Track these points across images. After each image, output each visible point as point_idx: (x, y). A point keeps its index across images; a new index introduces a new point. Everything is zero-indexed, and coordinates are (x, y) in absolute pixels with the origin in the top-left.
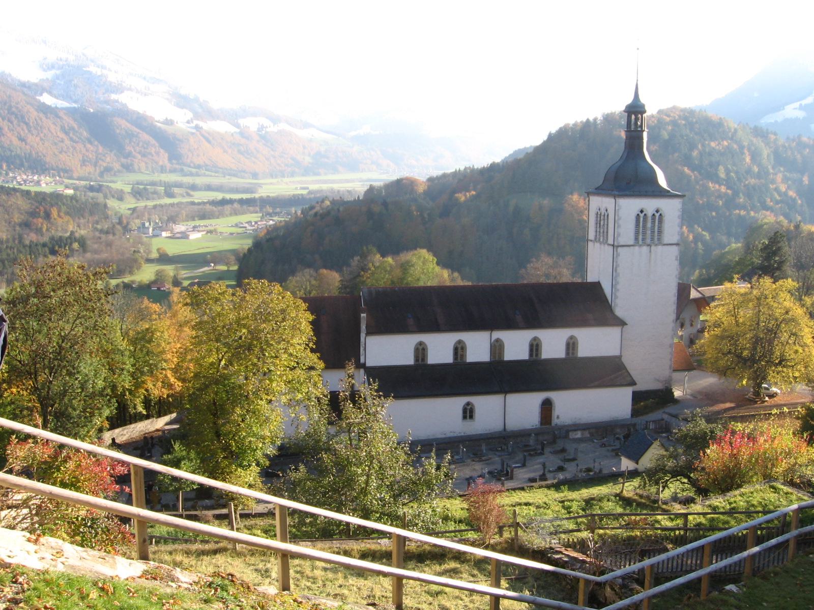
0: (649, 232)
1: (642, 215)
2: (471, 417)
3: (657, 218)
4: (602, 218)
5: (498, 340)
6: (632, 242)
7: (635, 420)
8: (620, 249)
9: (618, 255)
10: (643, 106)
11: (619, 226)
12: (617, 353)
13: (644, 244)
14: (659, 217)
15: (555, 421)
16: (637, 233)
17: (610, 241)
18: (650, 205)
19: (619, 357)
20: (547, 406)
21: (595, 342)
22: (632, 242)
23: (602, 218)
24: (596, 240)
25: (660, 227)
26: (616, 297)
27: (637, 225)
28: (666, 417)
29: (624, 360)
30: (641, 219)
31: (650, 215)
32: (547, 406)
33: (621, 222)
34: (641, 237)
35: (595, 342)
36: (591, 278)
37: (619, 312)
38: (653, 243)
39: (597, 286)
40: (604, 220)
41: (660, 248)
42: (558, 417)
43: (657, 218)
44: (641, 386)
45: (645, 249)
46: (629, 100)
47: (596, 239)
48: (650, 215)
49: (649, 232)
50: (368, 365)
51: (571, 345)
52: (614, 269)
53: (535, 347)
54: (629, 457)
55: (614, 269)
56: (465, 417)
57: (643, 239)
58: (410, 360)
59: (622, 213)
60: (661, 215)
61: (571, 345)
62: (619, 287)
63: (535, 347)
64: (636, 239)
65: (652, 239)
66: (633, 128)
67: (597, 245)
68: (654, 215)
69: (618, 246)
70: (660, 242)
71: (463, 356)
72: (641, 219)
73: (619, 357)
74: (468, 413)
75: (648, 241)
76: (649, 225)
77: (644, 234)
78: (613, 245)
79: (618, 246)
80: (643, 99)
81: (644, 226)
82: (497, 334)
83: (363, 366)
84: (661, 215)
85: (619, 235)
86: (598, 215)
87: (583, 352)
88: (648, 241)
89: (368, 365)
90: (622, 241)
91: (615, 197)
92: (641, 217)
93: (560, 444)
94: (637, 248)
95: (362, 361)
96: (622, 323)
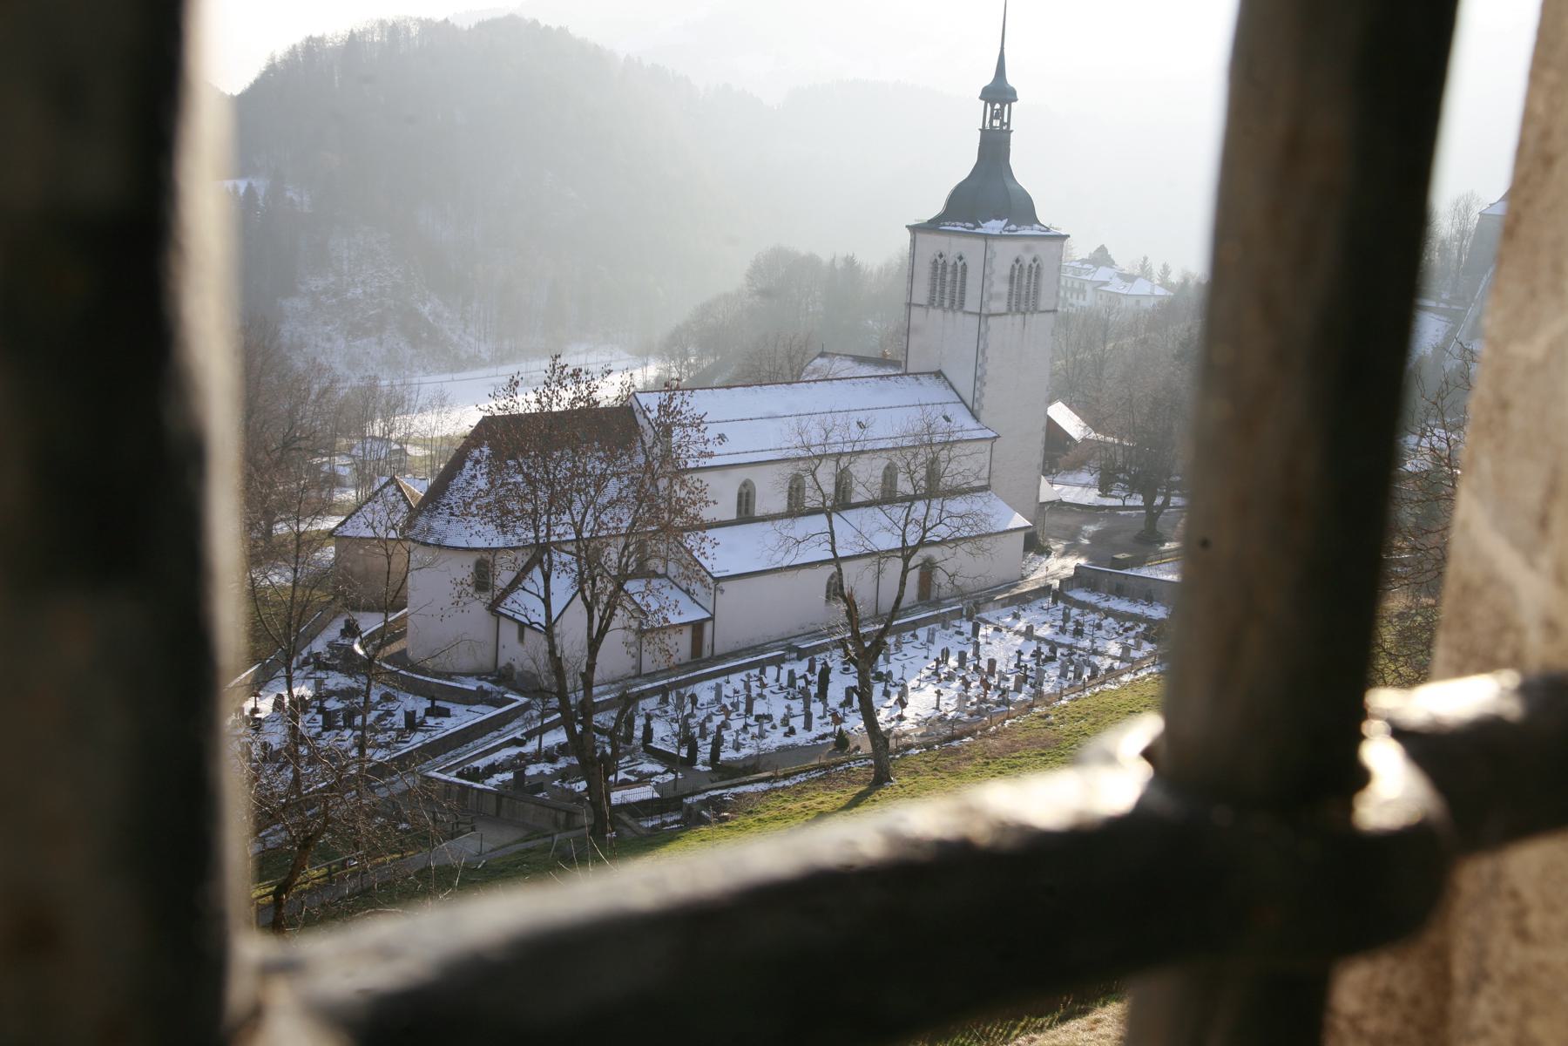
4: (949, 269)
8: (991, 320)
9: (988, 328)
10: (1013, 92)
13: (1018, 311)
17: (972, 304)
22: (1004, 309)
25: (1036, 284)
40: (955, 275)
45: (1019, 318)
46: (988, 78)
52: (980, 352)
55: (980, 352)
57: (1018, 303)
69: (988, 316)
70: (1036, 310)
76: (1025, 282)
78: (980, 314)
79: (988, 316)
80: (1011, 79)
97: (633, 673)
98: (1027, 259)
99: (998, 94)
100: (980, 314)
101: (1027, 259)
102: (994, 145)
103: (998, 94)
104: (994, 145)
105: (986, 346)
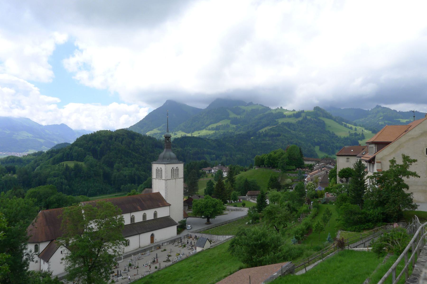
2: (128, 245)
5: (133, 216)
7: (179, 236)
14: (177, 169)
15: (155, 241)
16: (172, 175)
17: (164, 178)
18: (175, 166)
20: (152, 236)
21: (162, 212)
23: (159, 172)
24: (157, 178)
27: (172, 172)
28: (190, 233)
29: (171, 216)
32: (152, 236)
35: (162, 212)
36: (155, 190)
37: (168, 202)
39: (158, 194)
45: (174, 180)
47: (156, 177)
51: (155, 214)
53: (144, 216)
54: (200, 246)
55: (166, 187)
61: (155, 214)
63: (144, 216)
75: (175, 177)
76: (175, 172)
77: (174, 175)
82: (133, 214)
86: (157, 170)
87: (159, 216)
88: (175, 177)
91: (165, 164)
93: (163, 248)
96: (170, 205)
98: (175, 168)
101: (175, 168)
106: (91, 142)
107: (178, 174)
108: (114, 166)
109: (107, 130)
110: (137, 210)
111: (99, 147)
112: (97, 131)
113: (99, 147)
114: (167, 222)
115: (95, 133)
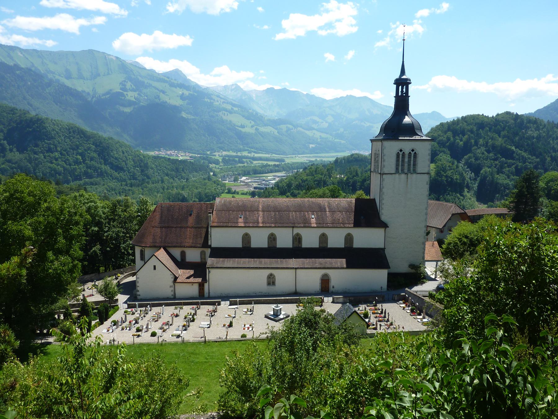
0: (406, 165)
1: (401, 153)
2: (274, 283)
3: (412, 155)
5: (298, 234)
6: (394, 172)
8: (384, 176)
9: (383, 180)
11: (384, 161)
12: (382, 246)
14: (413, 155)
16: (397, 165)
19: (383, 250)
22: (394, 172)
25: (415, 162)
26: (382, 209)
29: (386, 252)
30: (401, 156)
31: (407, 153)
33: (385, 158)
34: (400, 168)
35: (367, 238)
38: (410, 172)
41: (415, 175)
42: (333, 287)
43: (412, 155)
44: (394, 270)
45: (403, 176)
48: (407, 153)
49: (406, 165)
50: (212, 246)
56: (269, 284)
58: (239, 245)
59: (385, 151)
60: (415, 153)
61: (349, 238)
62: (383, 202)
64: (397, 169)
65: (409, 170)
66: (400, 94)
67: (375, 174)
68: (410, 153)
69: (383, 174)
70: (415, 172)
71: (249, 242)
72: (401, 156)
73: (383, 250)
74: (271, 280)
75: (406, 171)
76: (406, 160)
78: (380, 174)
79: (383, 174)
81: (403, 161)
82: (296, 231)
83: (210, 247)
84: (415, 153)
85: (384, 166)
87: (358, 243)
88: (406, 171)
89: (212, 246)
90: (386, 170)
92: (400, 155)
94: (397, 175)
95: (209, 243)
96: (384, 225)
97: (172, 297)
99: (402, 83)
100: (380, 174)
102: (402, 103)
103: (402, 83)
104: (402, 103)
105: (383, 188)
106: (450, 134)
107: (415, 165)
108: (482, 172)
109: (479, 115)
110: (307, 224)
111: (461, 140)
112: (463, 117)
113: (461, 140)
114: (372, 258)
115: (458, 120)
